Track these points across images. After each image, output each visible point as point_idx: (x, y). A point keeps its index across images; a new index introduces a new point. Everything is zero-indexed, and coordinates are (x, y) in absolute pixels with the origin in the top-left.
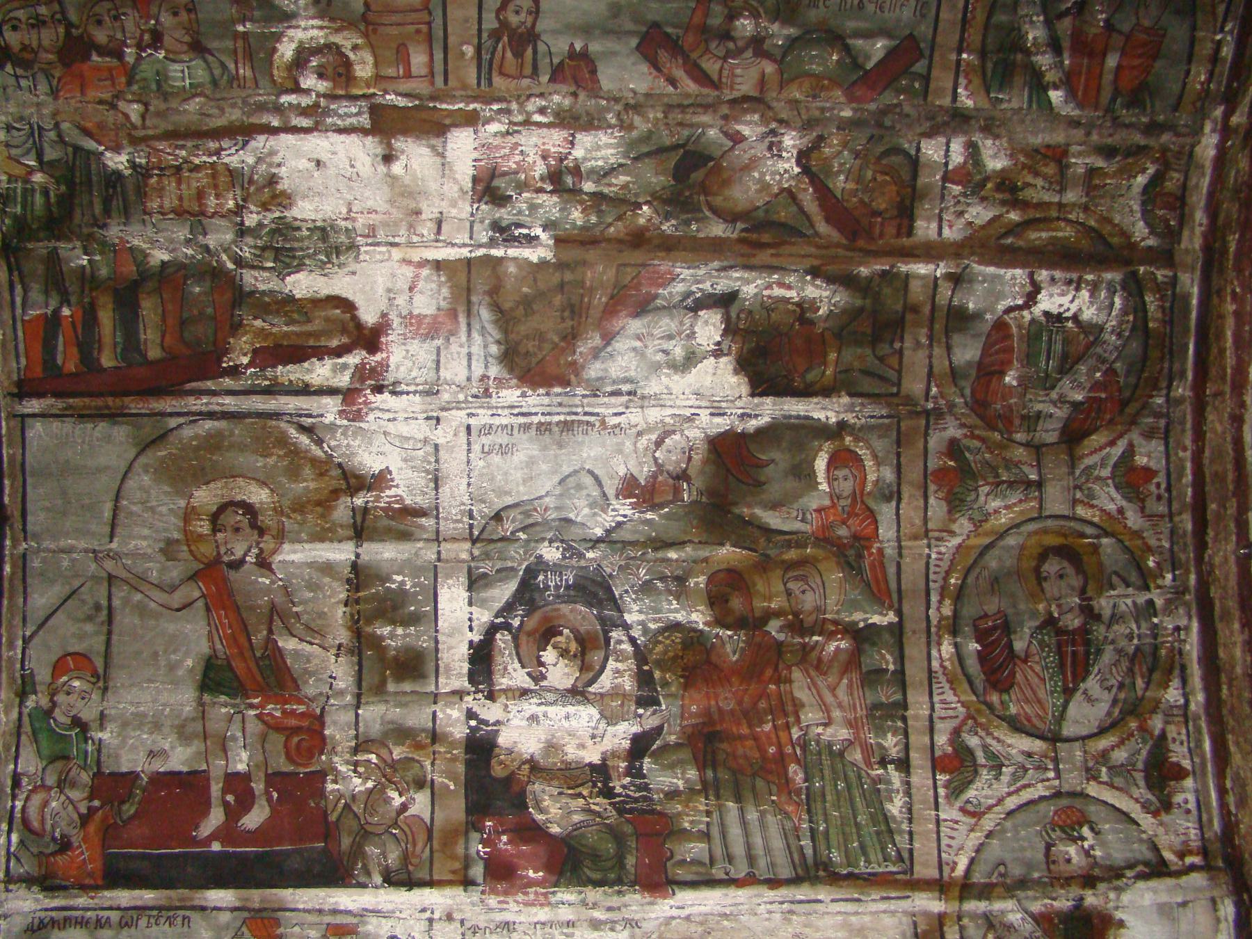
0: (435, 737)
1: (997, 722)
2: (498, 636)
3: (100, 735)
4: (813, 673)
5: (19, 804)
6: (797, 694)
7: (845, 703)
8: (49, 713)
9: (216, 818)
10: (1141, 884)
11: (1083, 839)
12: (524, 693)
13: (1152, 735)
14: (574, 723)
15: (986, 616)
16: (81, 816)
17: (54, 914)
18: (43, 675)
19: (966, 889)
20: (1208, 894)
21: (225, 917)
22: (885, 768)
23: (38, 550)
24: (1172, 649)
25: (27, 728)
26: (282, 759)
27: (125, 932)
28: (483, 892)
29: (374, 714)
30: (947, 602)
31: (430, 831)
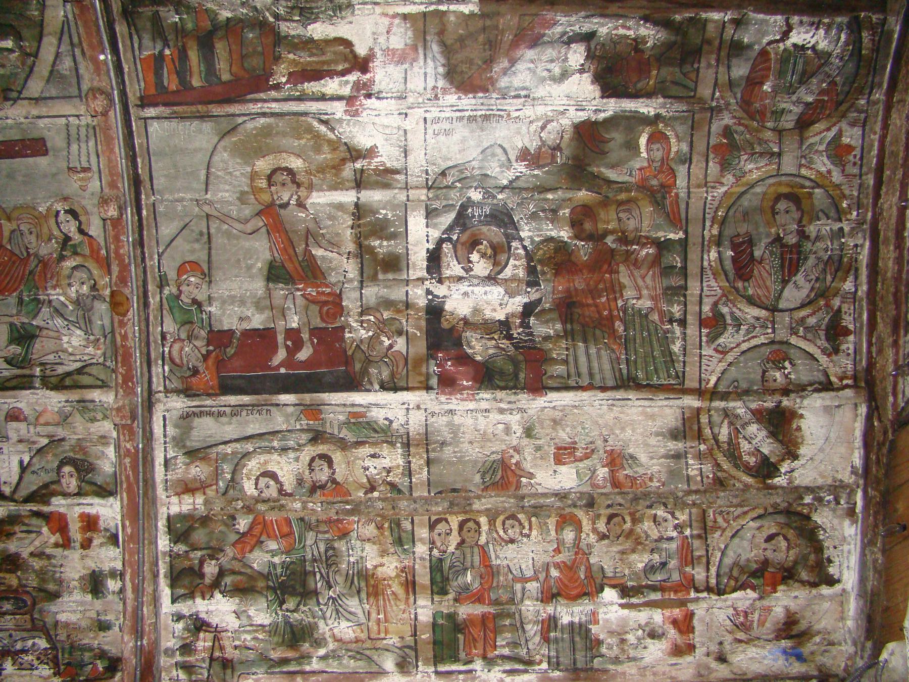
0: (408, 305)
1: (740, 299)
2: (444, 245)
3: (210, 309)
4: (632, 268)
5: (167, 350)
6: (622, 280)
7: (650, 286)
8: (178, 297)
9: (282, 354)
10: (815, 395)
11: (785, 368)
12: (460, 279)
13: (832, 309)
14: (489, 297)
15: (739, 235)
17: (194, 409)
18: (172, 275)
19: (714, 394)
20: (853, 402)
21: (290, 409)
22: (672, 325)
23: (162, 201)
24: (851, 258)
25: (166, 306)
26: (319, 320)
27: (234, 418)
28: (437, 394)
29: (372, 293)
30: (716, 226)
31: (406, 360)
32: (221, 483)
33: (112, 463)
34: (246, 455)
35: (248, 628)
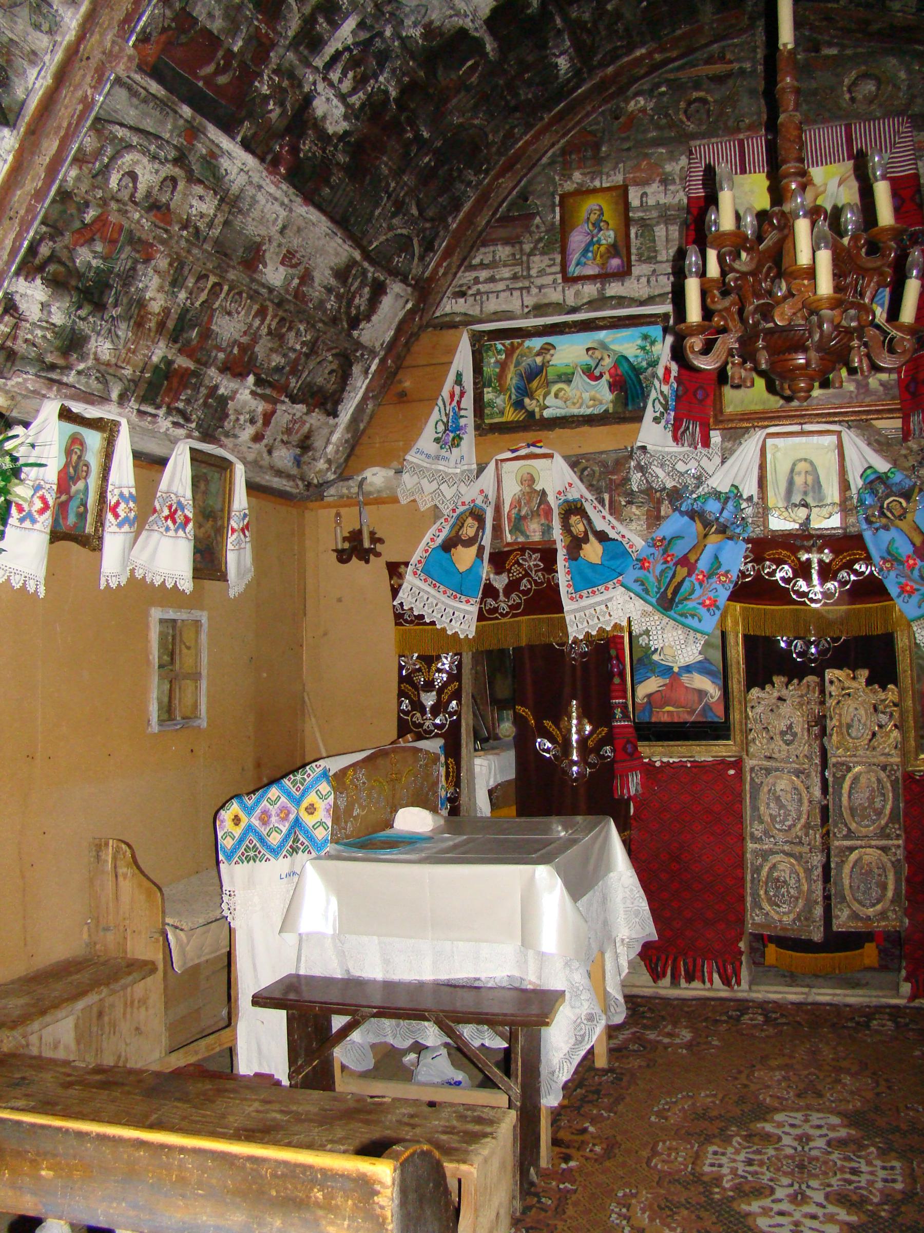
9: (210, 69)
16: (163, 27)
21: (181, 122)
32: (97, 164)
33: (27, 89)
34: (129, 147)
35: (44, 324)
